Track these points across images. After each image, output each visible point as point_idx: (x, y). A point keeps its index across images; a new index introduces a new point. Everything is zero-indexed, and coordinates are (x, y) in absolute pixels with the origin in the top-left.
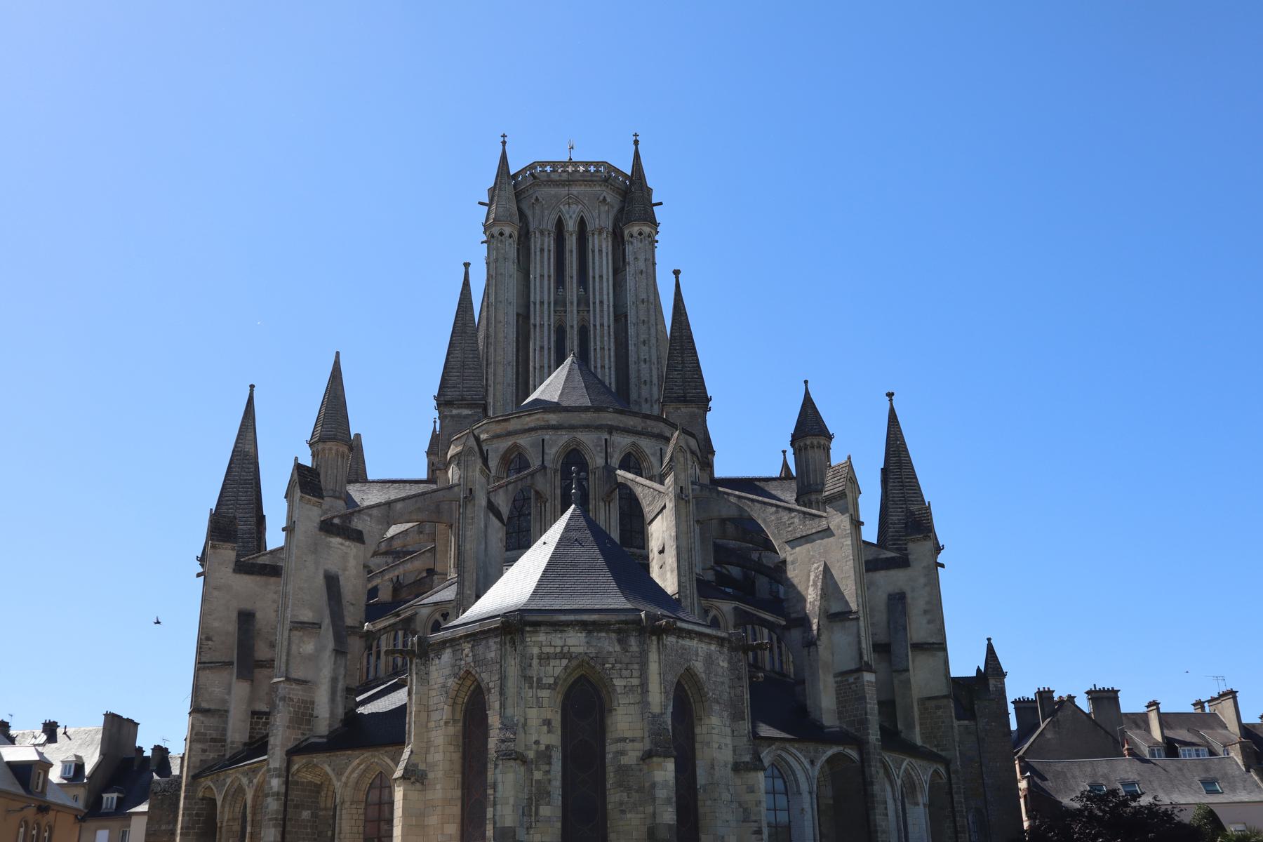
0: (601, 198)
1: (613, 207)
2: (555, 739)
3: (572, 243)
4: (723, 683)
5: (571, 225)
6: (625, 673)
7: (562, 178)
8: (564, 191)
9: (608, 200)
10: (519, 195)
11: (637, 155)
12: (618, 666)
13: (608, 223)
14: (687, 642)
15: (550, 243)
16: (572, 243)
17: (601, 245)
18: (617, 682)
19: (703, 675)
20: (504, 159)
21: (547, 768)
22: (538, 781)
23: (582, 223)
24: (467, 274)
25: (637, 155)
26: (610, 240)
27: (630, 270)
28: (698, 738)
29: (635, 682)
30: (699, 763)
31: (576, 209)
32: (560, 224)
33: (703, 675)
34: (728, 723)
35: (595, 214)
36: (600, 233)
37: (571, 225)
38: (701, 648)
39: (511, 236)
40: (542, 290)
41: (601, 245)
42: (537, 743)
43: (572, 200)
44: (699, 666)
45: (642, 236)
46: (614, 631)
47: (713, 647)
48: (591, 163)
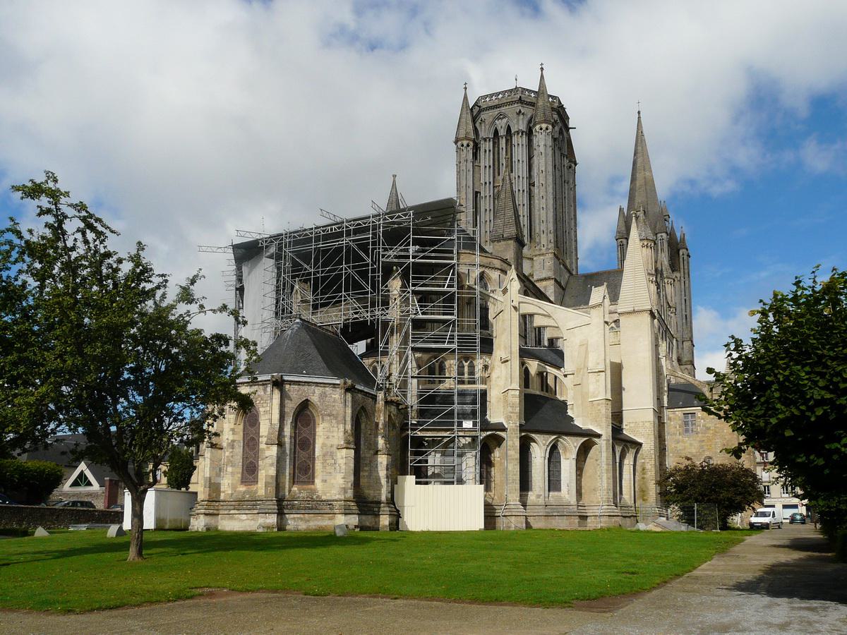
0: (518, 111)
1: (527, 115)
2: (240, 437)
3: (503, 142)
4: (334, 406)
5: (502, 132)
6: (265, 405)
7: (495, 104)
8: (496, 112)
9: (523, 112)
10: (474, 120)
11: (542, 76)
12: (262, 402)
13: (522, 126)
14: (306, 388)
15: (488, 146)
16: (503, 142)
17: (520, 141)
18: (261, 409)
19: (318, 403)
20: (466, 98)
21: (231, 450)
22: (227, 457)
23: (509, 129)
24: (394, 181)
25: (542, 76)
26: (524, 136)
27: (535, 153)
28: (317, 434)
29: (268, 409)
30: (317, 446)
31: (505, 120)
32: (496, 132)
33: (318, 403)
34: (335, 426)
35: (515, 121)
36: (518, 134)
37: (502, 132)
38: (318, 390)
39: (468, 145)
40: (485, 176)
41: (520, 141)
42: (227, 439)
43: (501, 116)
44: (315, 399)
45: (548, 131)
46: (261, 385)
47: (327, 389)
48: (500, 93)
